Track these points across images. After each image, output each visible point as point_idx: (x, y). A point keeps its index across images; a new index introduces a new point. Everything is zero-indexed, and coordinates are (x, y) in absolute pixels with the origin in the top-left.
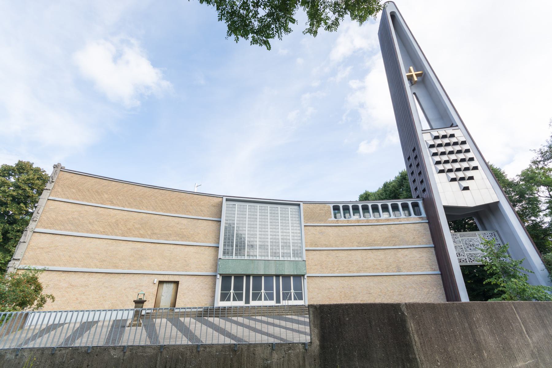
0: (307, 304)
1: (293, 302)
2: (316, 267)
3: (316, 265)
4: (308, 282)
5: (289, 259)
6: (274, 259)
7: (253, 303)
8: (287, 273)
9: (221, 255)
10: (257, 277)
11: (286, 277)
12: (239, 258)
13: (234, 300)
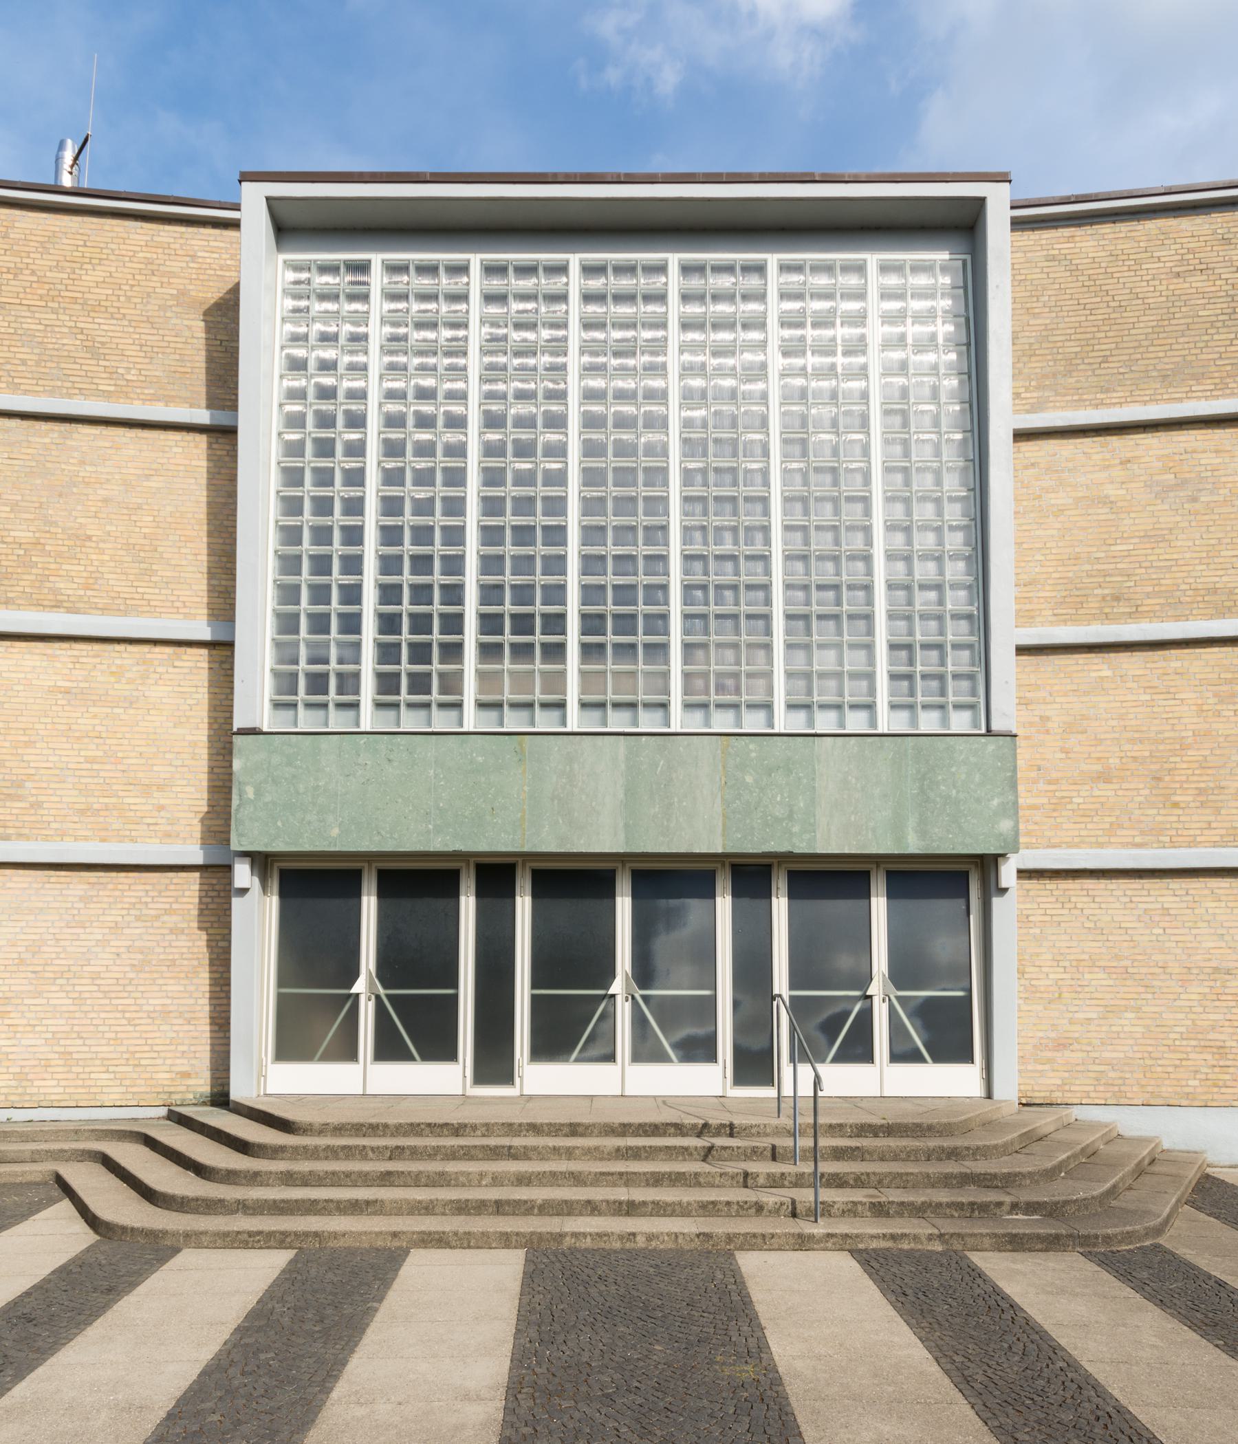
0: (1008, 1089)
1: (881, 1082)
2: (1104, 791)
3: (1104, 777)
4: (1024, 920)
5: (856, 722)
6: (722, 722)
7: (541, 1080)
8: (831, 837)
9: (255, 702)
10: (574, 882)
11: (830, 880)
12: (410, 721)
13: (389, 1049)
